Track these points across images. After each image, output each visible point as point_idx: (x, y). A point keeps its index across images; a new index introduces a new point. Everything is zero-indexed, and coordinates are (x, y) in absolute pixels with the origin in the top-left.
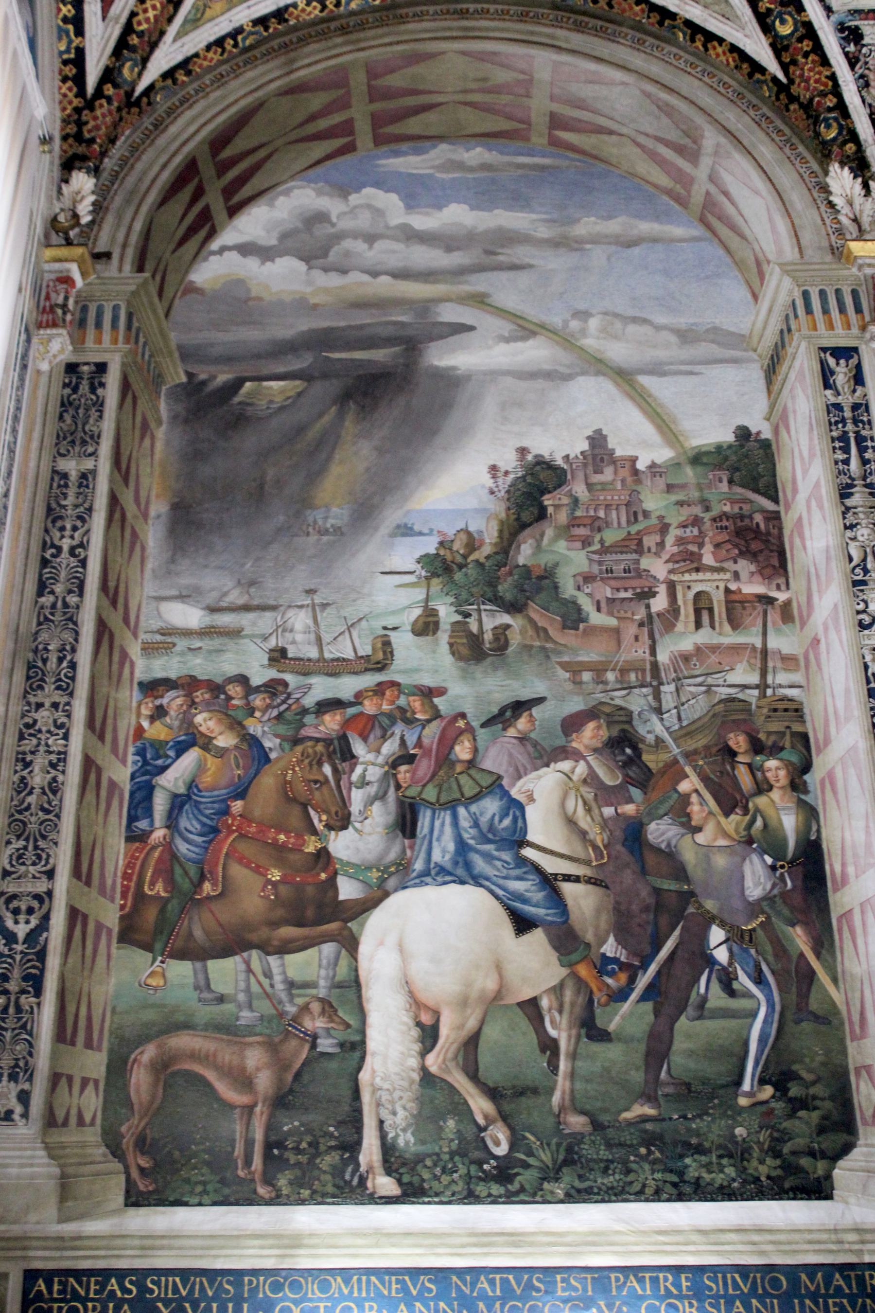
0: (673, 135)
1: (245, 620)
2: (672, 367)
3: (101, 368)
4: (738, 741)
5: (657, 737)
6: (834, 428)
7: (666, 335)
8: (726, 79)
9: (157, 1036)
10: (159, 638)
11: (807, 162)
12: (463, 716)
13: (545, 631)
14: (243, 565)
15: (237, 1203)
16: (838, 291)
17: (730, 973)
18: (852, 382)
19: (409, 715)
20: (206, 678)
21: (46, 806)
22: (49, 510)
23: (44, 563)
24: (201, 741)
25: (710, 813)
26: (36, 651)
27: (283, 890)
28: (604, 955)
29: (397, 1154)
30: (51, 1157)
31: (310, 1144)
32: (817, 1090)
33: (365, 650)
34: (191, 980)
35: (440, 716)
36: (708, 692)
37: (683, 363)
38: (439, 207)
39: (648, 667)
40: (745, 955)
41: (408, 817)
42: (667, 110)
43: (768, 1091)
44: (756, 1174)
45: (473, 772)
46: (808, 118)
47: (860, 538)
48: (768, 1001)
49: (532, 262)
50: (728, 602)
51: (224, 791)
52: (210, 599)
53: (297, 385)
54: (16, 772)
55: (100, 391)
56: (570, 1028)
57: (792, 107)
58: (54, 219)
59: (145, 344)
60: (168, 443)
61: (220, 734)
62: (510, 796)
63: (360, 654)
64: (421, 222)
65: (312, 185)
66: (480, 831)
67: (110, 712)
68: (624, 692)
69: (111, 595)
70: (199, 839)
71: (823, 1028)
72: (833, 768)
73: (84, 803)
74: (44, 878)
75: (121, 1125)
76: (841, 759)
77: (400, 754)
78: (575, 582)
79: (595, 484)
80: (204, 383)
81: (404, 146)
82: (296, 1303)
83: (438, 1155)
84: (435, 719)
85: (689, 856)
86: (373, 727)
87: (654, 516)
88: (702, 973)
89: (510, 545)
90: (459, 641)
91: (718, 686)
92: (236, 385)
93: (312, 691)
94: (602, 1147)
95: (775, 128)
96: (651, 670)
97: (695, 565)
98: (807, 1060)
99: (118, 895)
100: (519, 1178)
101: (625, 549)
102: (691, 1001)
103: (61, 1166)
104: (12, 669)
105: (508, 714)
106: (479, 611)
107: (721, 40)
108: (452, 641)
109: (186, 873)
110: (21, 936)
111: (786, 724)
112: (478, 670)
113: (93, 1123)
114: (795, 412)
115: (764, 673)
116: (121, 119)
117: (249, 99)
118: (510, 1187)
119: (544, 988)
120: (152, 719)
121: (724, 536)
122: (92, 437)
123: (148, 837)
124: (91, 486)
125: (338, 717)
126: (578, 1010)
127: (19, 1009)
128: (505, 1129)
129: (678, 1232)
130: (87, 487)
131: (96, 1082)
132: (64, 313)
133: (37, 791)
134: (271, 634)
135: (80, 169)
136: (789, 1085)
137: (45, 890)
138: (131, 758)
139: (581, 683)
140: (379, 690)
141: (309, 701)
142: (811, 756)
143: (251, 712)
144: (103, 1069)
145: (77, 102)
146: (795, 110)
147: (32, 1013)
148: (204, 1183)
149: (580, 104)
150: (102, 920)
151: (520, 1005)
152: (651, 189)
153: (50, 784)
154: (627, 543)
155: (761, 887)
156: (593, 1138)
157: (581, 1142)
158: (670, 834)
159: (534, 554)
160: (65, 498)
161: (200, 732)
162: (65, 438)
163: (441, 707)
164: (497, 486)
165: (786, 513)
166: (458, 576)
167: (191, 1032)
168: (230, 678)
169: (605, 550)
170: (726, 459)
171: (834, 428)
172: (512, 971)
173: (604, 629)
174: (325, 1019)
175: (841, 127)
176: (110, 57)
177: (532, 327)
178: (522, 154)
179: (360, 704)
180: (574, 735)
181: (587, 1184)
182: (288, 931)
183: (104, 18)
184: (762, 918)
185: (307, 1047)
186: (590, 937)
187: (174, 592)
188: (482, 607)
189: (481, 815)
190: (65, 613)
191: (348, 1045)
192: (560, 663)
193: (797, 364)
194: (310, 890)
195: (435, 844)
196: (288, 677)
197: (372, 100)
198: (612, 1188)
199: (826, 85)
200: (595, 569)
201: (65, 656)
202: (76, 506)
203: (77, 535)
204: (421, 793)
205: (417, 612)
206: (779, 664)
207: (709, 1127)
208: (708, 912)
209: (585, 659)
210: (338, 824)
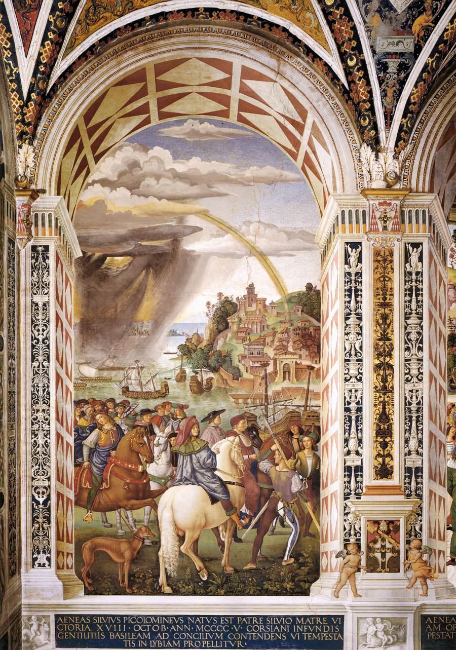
1: (113, 373)
3: (47, 248)
4: (295, 429)
6: (346, 284)
9: (91, 539)
10: (80, 382)
12: (195, 417)
13: (226, 380)
14: (110, 349)
15: (120, 594)
16: (357, 211)
19: (175, 416)
21: (44, 452)
22: (32, 321)
23: (33, 347)
24: (99, 426)
25: (282, 458)
26: (34, 386)
27: (131, 486)
32: (309, 560)
33: (158, 388)
34: (101, 519)
38: (188, 159)
43: (293, 560)
45: (198, 440)
47: (350, 340)
49: (230, 193)
52: (98, 364)
54: (32, 438)
55: (47, 261)
56: (228, 538)
60: (77, 287)
64: (181, 167)
66: (200, 464)
70: (101, 466)
73: (58, 452)
80: (90, 257)
82: (140, 625)
85: (273, 476)
87: (271, 327)
89: (214, 340)
92: (102, 259)
97: (285, 351)
98: (306, 550)
100: (210, 588)
105: (211, 416)
106: (201, 371)
107: (321, 59)
109: (97, 479)
110: (41, 503)
112: (201, 397)
113: (72, 568)
115: (307, 400)
121: (297, 338)
122: (46, 285)
127: (43, 529)
130: (46, 309)
131: (72, 554)
133: (41, 446)
139: (238, 403)
140: (164, 405)
141: (138, 410)
143: (116, 415)
144: (74, 550)
148: (110, 588)
150: (68, 496)
153: (45, 443)
162: (35, 285)
166: (193, 355)
171: (346, 284)
176: (32, 78)
182: (134, 502)
183: (26, 57)
185: (141, 543)
186: (237, 505)
190: (43, 370)
195: (184, 469)
196: (130, 400)
197: (157, 91)
200: (246, 353)
202: (43, 320)
203: (45, 333)
205: (178, 371)
209: (241, 393)
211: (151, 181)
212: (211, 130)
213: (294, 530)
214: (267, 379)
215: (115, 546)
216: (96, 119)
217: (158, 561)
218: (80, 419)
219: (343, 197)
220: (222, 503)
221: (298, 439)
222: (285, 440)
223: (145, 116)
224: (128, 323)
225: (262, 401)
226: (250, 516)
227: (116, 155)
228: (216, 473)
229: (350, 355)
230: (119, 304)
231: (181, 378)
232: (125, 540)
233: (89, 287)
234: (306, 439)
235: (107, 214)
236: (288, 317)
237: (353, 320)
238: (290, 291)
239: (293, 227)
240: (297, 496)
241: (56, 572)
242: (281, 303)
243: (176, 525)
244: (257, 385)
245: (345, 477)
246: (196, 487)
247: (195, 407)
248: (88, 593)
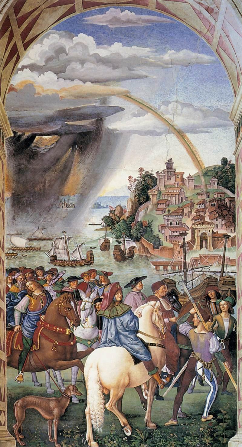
1: (42, 243)
2: (200, 129)
4: (212, 294)
10: (11, 251)
12: (118, 283)
14: (39, 221)
17: (202, 378)
25: (200, 321)
29: (97, 435)
31: (71, 432)
32: (227, 416)
33: (84, 257)
34: (31, 379)
35: (110, 283)
38: (110, 45)
39: (183, 264)
40: (208, 372)
41: (100, 322)
43: (211, 416)
44: (205, 442)
45: (121, 305)
48: (214, 387)
49: (148, 75)
50: (212, 237)
51: (37, 312)
52: (28, 235)
61: (35, 290)
62: (134, 314)
63: (82, 259)
64: (104, 52)
68: (175, 274)
70: (31, 329)
71: (230, 397)
75: (13, 425)
77: (97, 298)
80: (20, 137)
85: (192, 338)
86: (88, 287)
87: (189, 199)
88: (194, 378)
90: (117, 253)
91: (207, 272)
92: (32, 138)
94: (159, 433)
96: (184, 265)
99: (6, 350)
100: (133, 443)
101: (178, 214)
105: (134, 282)
108: (115, 253)
111: (229, 287)
112: (124, 265)
113: (4, 425)
118: (131, 445)
123: (14, 329)
125: (75, 284)
126: (153, 390)
128: (130, 428)
131: (4, 412)
134: (51, 250)
141: (65, 277)
148: (39, 443)
156: (156, 430)
163: (110, 280)
166: (116, 226)
167: (32, 396)
168: (37, 268)
172: (133, 378)
180: (156, 292)
186: (158, 365)
187: (15, 232)
188: (125, 239)
191: (82, 400)
192: (151, 262)
196: (58, 268)
200: (166, 223)
205: (102, 241)
206: (229, 264)
207: (192, 427)
209: (161, 261)
211: (76, 66)
212: (131, 18)
213: (212, 388)
214: (186, 247)
217: (85, 417)
218: (12, 285)
220: (144, 363)
221: (215, 303)
222: (203, 304)
224: (56, 197)
225: (181, 268)
226: (171, 375)
227: (44, 42)
228: (139, 335)
230: (48, 179)
231: (105, 247)
232: (54, 398)
233: (19, 164)
234: (223, 302)
235: (36, 96)
236: (205, 190)
238: (206, 166)
239: (209, 105)
240: (215, 357)
243: (101, 384)
244: (176, 252)
247: (118, 274)
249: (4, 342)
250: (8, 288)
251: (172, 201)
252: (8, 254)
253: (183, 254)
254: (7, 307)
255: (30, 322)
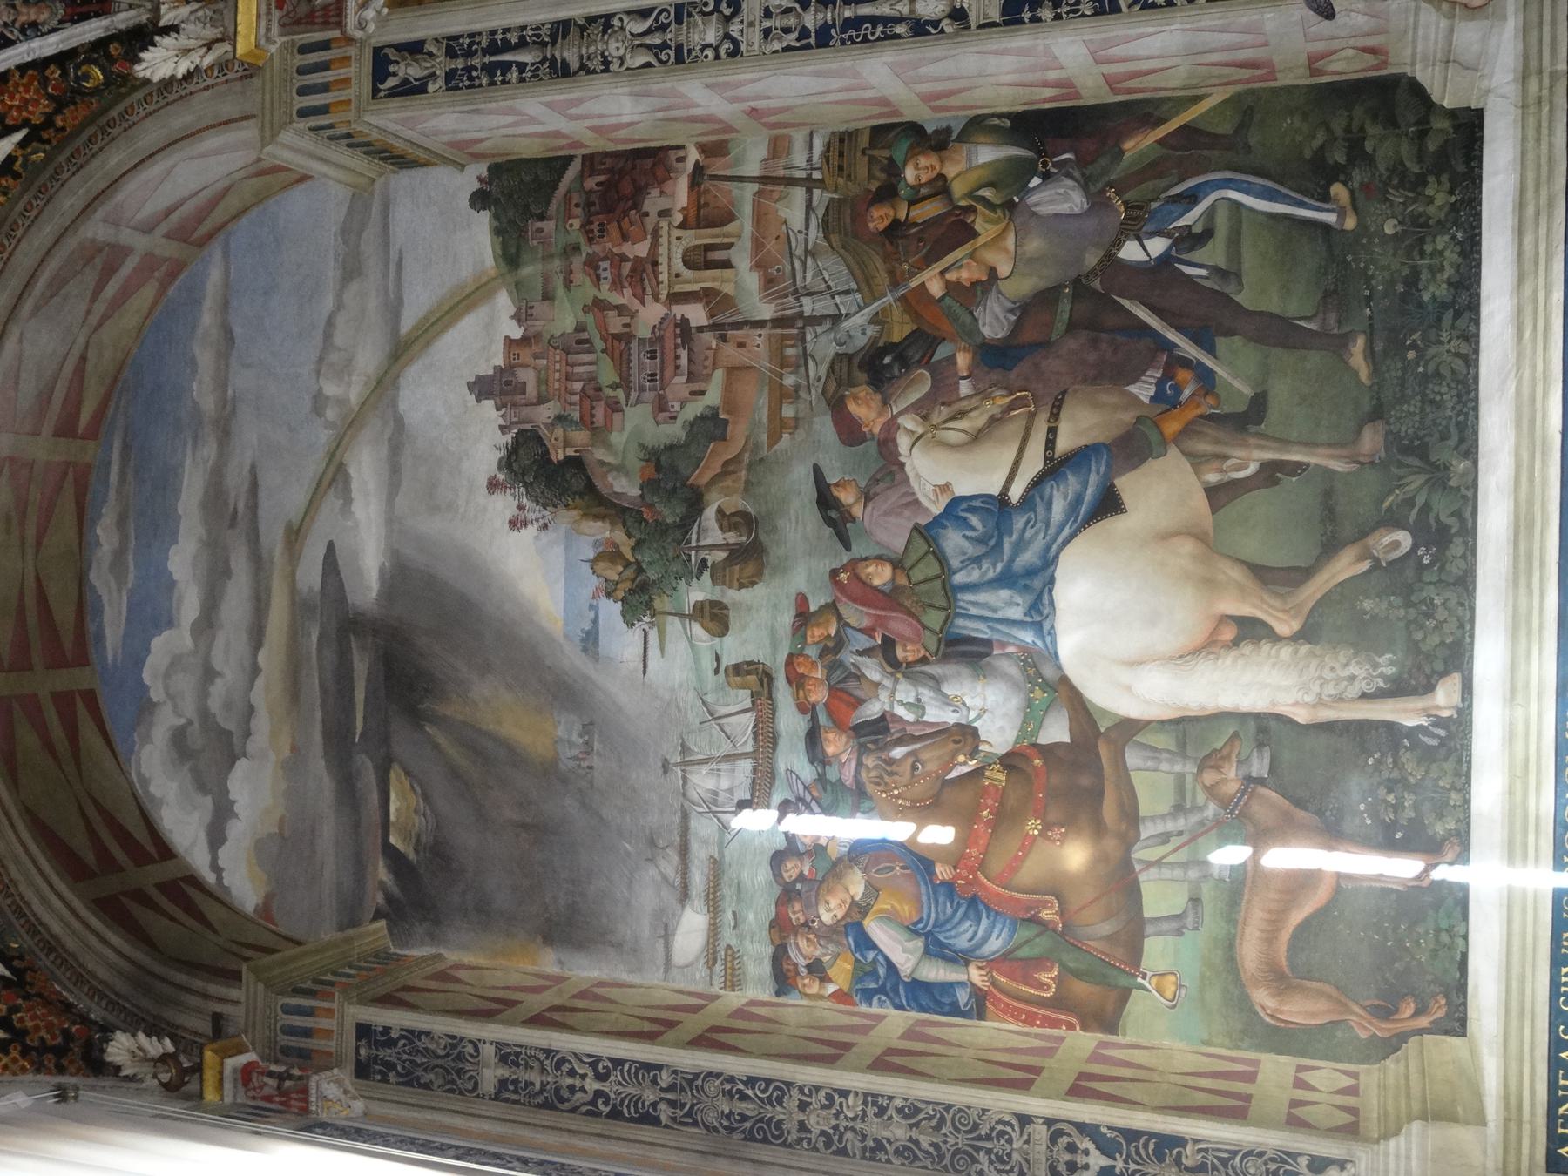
0: (90, 277)
3: (363, 1031)
4: (879, 218)
5: (871, 322)
6: (477, 82)
7: (349, 296)
8: (20, 207)
9: (1242, 986)
10: (719, 967)
11: (132, 106)
12: (834, 573)
13: (727, 463)
14: (628, 854)
18: (419, 56)
19: (830, 644)
20: (773, 906)
21: (935, 1121)
22: (547, 1106)
23: (615, 1114)
24: (856, 917)
25: (972, 256)
26: (730, 1129)
27: (1053, 815)
28: (1152, 399)
30: (1397, 1133)
31: (1390, 791)
32: (1338, 126)
33: (743, 698)
34: (1169, 938)
35: (834, 603)
36: (812, 253)
37: (385, 276)
38: (172, 584)
39: (779, 331)
40: (1159, 215)
42: (58, 284)
43: (1337, 189)
44: (1446, 209)
45: (908, 564)
46: (75, 103)
47: (622, 52)
49: (248, 462)
50: (698, 227)
51: (923, 889)
52: (669, 897)
53: (396, 776)
54: (888, 1161)
55: (394, 1035)
56: (1245, 446)
57: (59, 122)
58: (166, 1086)
59: (335, 973)
62: (941, 516)
64: (189, 606)
65: (136, 748)
67: (815, 1034)
68: (811, 363)
69: (662, 1029)
70: (985, 922)
72: (918, 95)
74: (1029, 1128)
75: (1357, 1037)
76: (906, 84)
78: (665, 422)
79: (539, 393)
80: (390, 899)
81: (91, 628)
83: (1409, 623)
84: (837, 610)
86: (842, 690)
88: (1183, 274)
89: (615, 505)
90: (736, 576)
91: (806, 241)
93: (795, 769)
94: (1405, 407)
95: (86, 146)
97: (649, 267)
98: (1299, 138)
99: (1055, 1032)
100: (1443, 518)
101: (625, 356)
102: (1218, 288)
103: (1410, 1119)
104: (753, 1161)
105: (833, 514)
106: (698, 548)
108: (736, 583)
109: (1026, 942)
110: (1105, 1161)
111: (859, 154)
112: (775, 552)
114: (454, 132)
115: (792, 182)
116: (39, 995)
117: (21, 826)
118: (1454, 530)
119: (1193, 478)
120: (825, 979)
121: (613, 229)
122: (453, 1046)
123: (980, 989)
124: (518, 1050)
125: (831, 736)
128: (1377, 534)
129: (1520, 311)
130: (518, 1055)
131: (1300, 1069)
132: (290, 1077)
133: (914, 1134)
135: (103, 1051)
136: (1331, 162)
137: (1045, 1127)
138: (875, 1009)
139: (796, 419)
140: (797, 681)
142: (901, 124)
144: (1283, 1059)
145: (14, 1054)
146: (64, 120)
147: (1206, 1150)
148: (1438, 931)
149: (45, 397)
150: (1086, 1055)
151: (1215, 507)
152: (159, 308)
153: (906, 1117)
154: (617, 353)
155: (1071, 192)
156: (1392, 420)
157: (1397, 436)
158: (998, 310)
159: (627, 474)
160: (532, 1084)
161: (843, 918)
162: (453, 1082)
163: (822, 602)
164: (537, 520)
165: (586, 146)
166: (652, 574)
168: (774, 875)
169: (625, 383)
170: (511, 222)
171: (477, 82)
173: (728, 387)
174: (1227, 765)
175: (88, 61)
177: (332, 469)
178: (108, 474)
179: (814, 706)
180: (865, 430)
181: (1453, 429)
182: (1109, 810)
184: (1111, 193)
186: (1128, 417)
188: (693, 544)
189: (964, 554)
190: (683, 1089)
192: (771, 446)
193: (392, 127)
194: (1056, 780)
195: (1000, 615)
197: (30, 668)
198: (1459, 396)
199: (32, 78)
200: (649, 396)
201: (739, 1091)
202: (543, 1070)
204: (934, 632)
205: (697, 629)
206: (782, 161)
208: (1101, 261)
209: (765, 412)
210: (970, 740)
215: (1273, 895)
216: (79, 842)
218: (830, 980)
219: (267, 118)
220: (1120, 474)
223: (80, 705)
225: (790, 337)
229: (664, 46)
231: (715, 617)
234: (910, 174)
237: (570, 53)
238: (489, 261)
241: (1367, 1140)
242: (518, 288)
245: (1039, 20)
246: (1062, 571)
248: (1456, 1023)
249: (1027, 1035)
250: (839, 996)
251: (585, 376)
252: (728, 983)
253: (746, 331)
254: (904, 1010)
255: (959, 923)
